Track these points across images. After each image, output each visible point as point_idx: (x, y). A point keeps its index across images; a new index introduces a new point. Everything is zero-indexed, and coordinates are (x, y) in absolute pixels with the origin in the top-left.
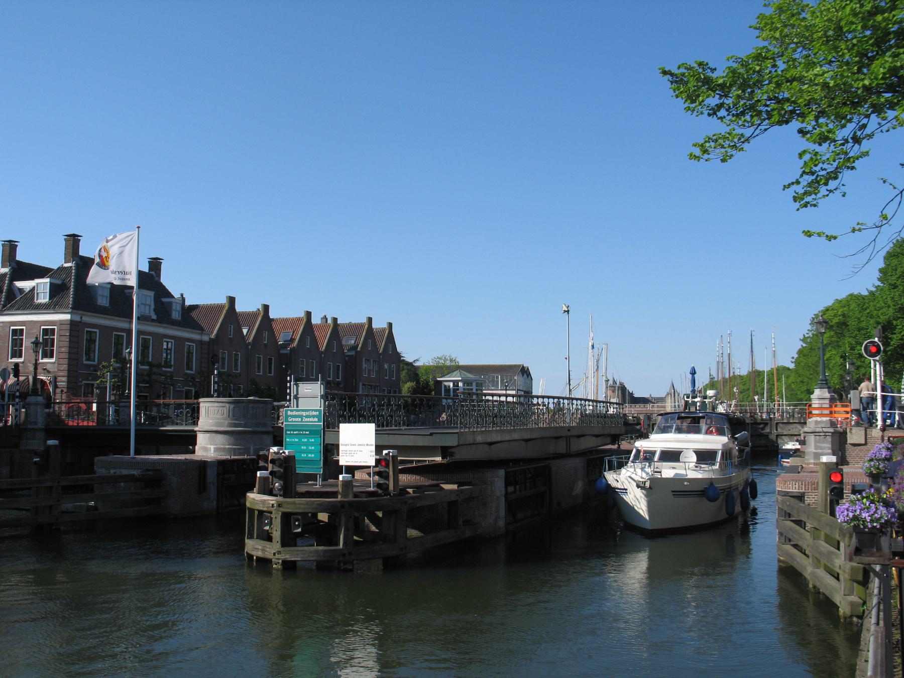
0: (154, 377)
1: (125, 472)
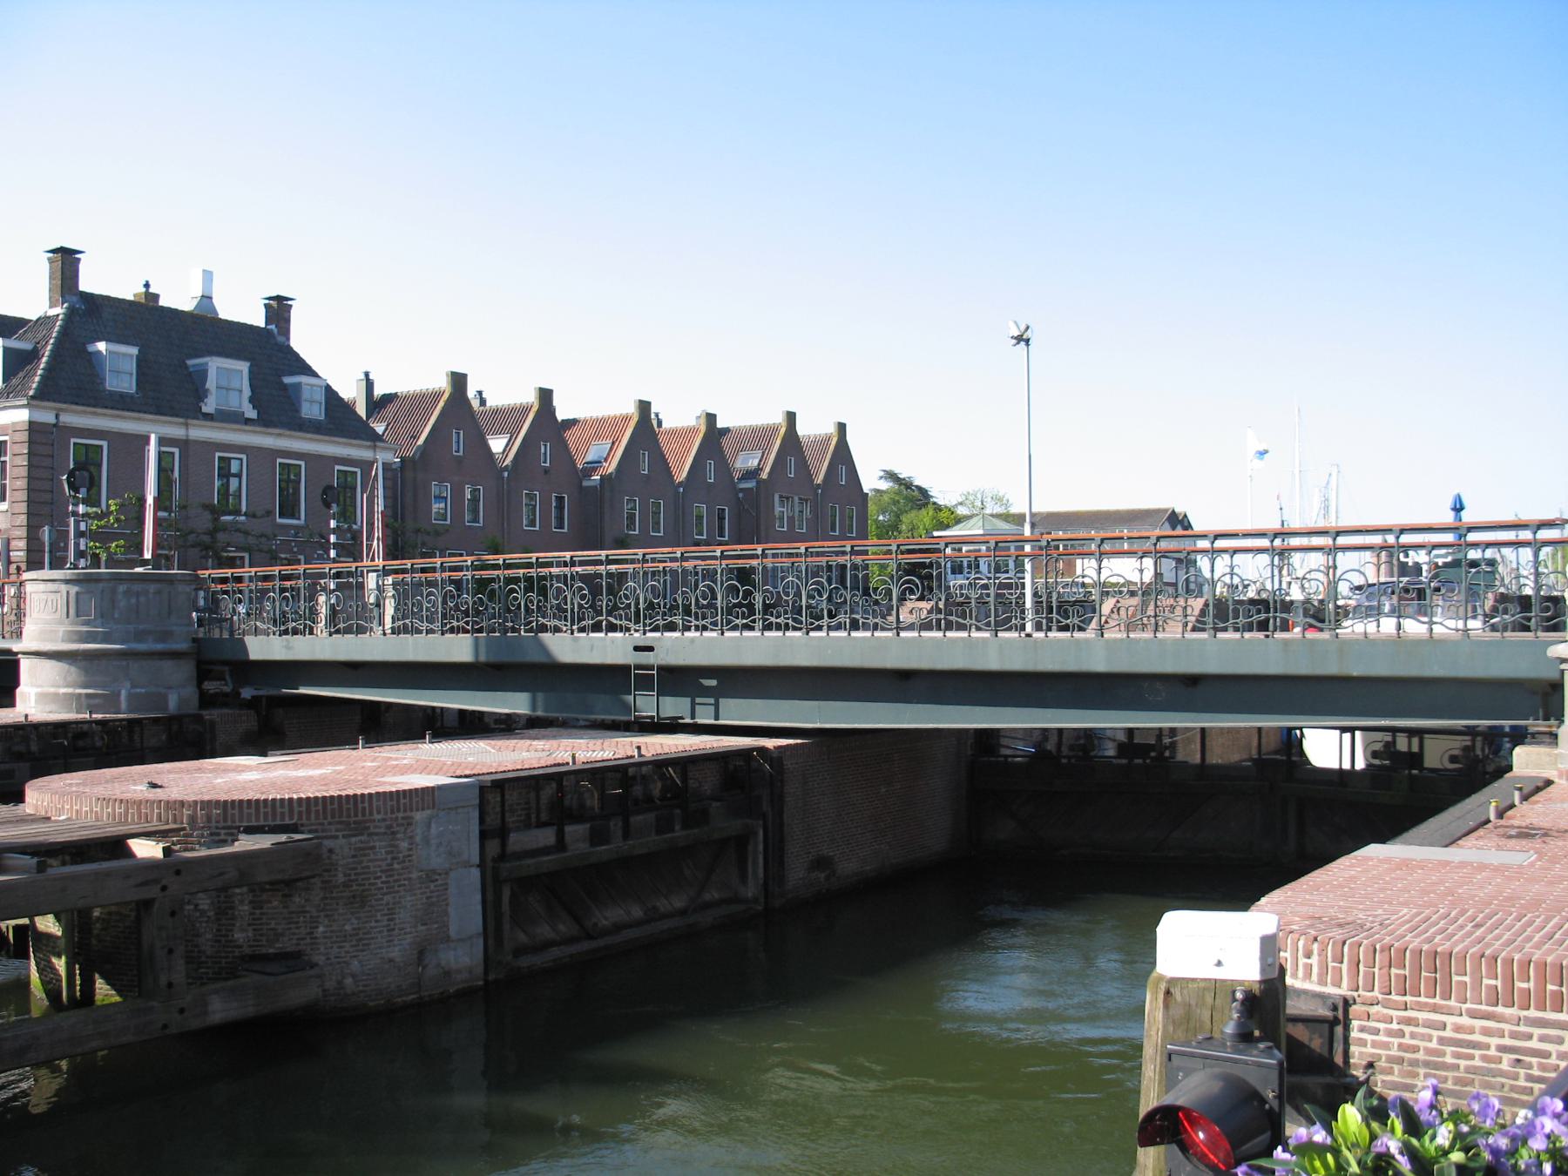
0: (222, 537)
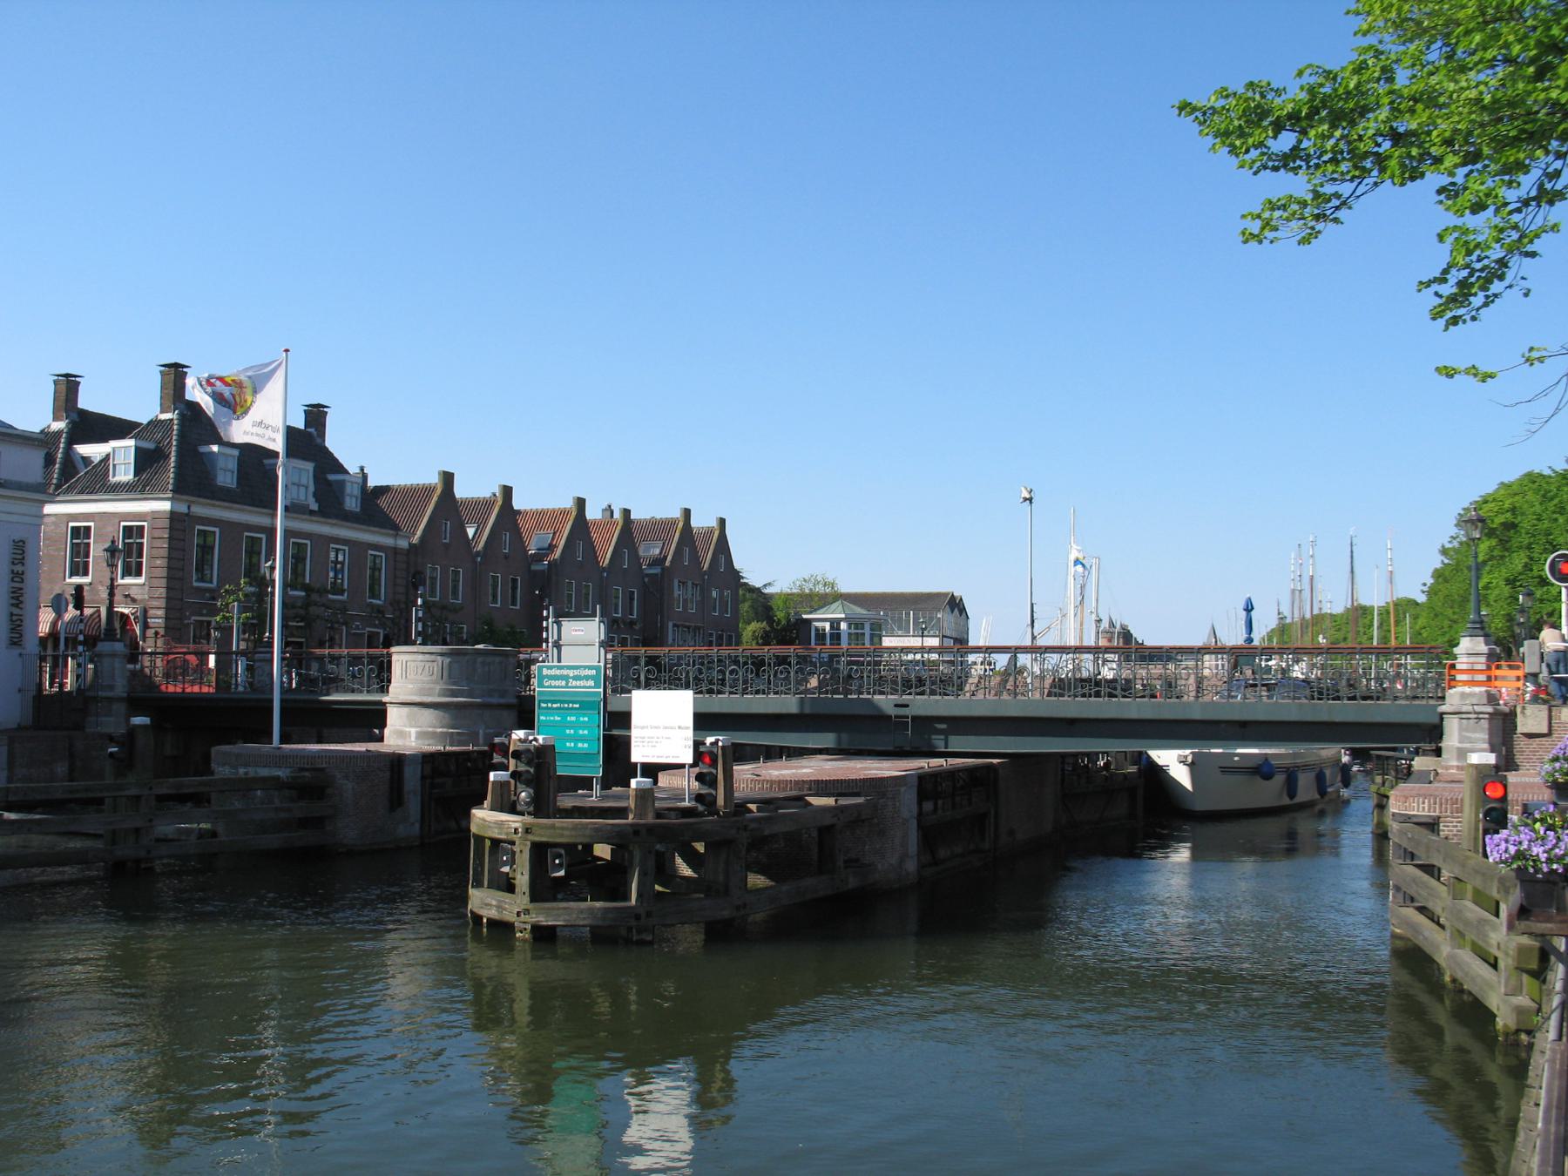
1: (264, 772)
